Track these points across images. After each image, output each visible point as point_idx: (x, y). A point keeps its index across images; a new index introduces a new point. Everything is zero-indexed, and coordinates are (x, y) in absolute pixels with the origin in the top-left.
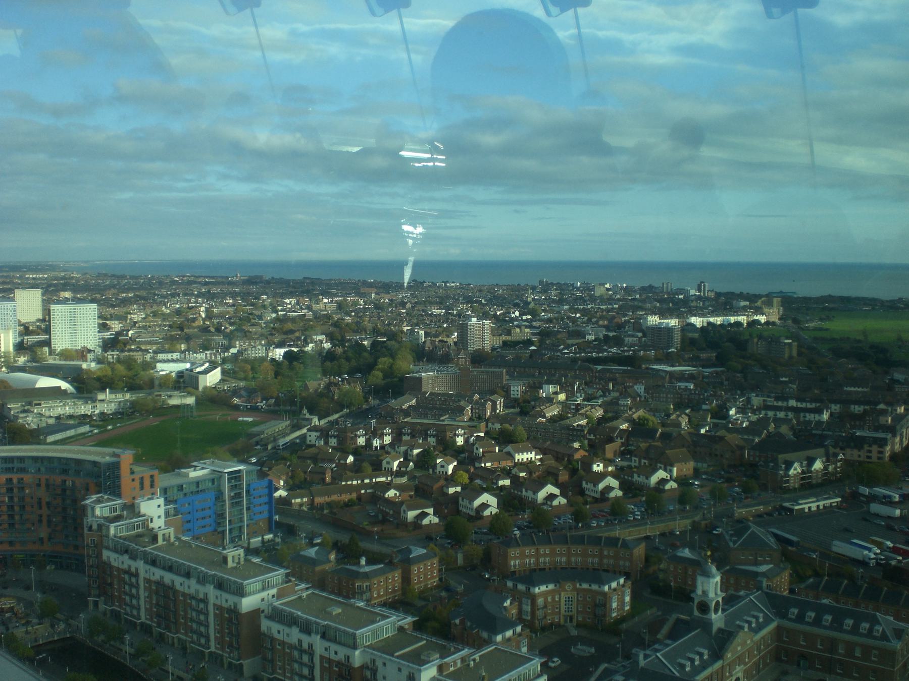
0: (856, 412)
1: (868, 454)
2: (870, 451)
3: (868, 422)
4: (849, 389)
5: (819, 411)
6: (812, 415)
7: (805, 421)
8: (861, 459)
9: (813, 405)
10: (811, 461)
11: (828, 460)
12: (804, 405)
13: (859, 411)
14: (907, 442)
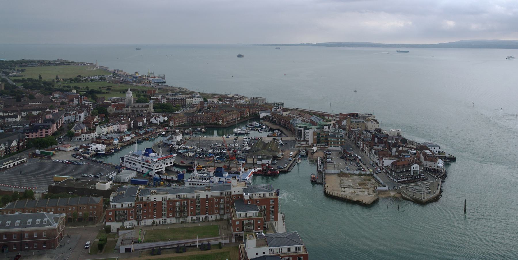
0: (35, 114)
1: (41, 134)
2: (42, 133)
3: (41, 118)
4: (31, 104)
5: (16, 116)
6: (12, 119)
7: (8, 122)
8: (37, 137)
9: (12, 114)
10: (11, 142)
11: (19, 140)
12: (7, 114)
13: (36, 114)
14: (60, 125)
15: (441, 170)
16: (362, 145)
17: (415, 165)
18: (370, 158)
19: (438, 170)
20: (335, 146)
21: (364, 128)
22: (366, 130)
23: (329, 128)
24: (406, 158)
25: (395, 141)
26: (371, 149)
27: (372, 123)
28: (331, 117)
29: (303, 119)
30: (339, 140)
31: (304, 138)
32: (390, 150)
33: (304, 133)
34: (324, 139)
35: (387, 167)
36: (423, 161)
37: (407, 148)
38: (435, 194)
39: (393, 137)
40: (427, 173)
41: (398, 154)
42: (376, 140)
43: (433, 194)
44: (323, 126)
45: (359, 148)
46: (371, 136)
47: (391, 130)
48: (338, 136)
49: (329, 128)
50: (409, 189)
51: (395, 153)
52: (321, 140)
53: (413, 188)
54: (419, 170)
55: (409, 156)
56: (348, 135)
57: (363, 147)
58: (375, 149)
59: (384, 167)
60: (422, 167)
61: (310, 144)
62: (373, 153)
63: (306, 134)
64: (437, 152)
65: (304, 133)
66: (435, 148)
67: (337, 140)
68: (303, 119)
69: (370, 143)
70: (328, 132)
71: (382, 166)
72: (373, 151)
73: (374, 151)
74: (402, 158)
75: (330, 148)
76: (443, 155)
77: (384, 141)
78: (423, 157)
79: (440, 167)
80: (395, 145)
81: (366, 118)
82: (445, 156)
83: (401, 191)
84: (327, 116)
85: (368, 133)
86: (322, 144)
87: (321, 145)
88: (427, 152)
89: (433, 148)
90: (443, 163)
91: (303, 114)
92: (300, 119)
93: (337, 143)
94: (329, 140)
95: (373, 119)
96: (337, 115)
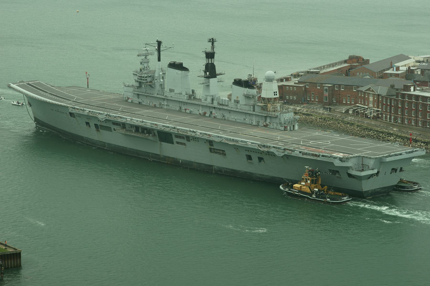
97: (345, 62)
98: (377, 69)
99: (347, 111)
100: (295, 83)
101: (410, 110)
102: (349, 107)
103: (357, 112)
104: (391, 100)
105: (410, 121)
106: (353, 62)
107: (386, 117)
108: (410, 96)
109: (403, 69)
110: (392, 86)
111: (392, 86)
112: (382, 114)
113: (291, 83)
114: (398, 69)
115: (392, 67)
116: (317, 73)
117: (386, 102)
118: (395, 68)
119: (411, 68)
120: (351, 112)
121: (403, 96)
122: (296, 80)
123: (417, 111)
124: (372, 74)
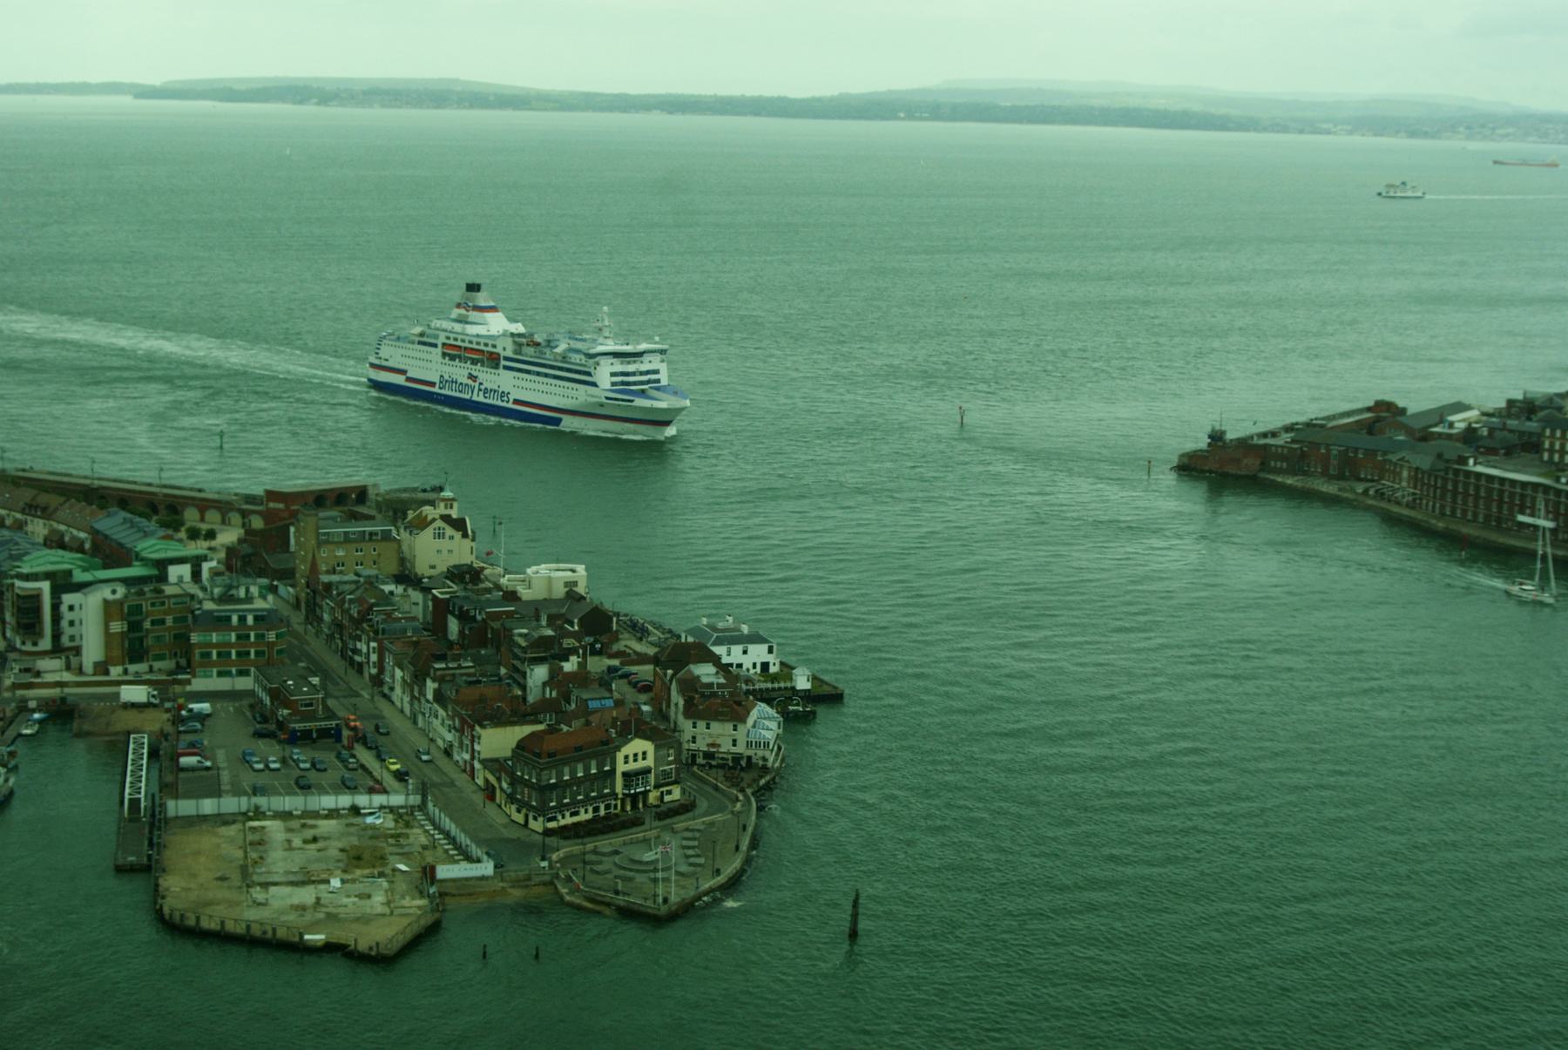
15: (765, 759)
16: (374, 657)
17: (638, 745)
18: (415, 722)
19: (749, 758)
20: (228, 674)
21: (393, 567)
22: (406, 577)
23: (196, 575)
24: (595, 711)
25: (549, 625)
26: (419, 678)
27: (439, 535)
28: (218, 509)
29: (53, 531)
30: (252, 639)
31: (56, 636)
32: (519, 677)
33: (56, 607)
34: (168, 637)
35: (493, 764)
36: (681, 718)
37: (611, 656)
38: (719, 878)
39: (536, 607)
40: (694, 775)
41: (554, 694)
42: (453, 626)
43: (713, 878)
44: (162, 565)
45: (359, 668)
46: (425, 607)
47: (534, 568)
48: (242, 619)
49: (196, 575)
50: (599, 863)
51: (541, 688)
52: (149, 642)
53: (617, 859)
54: (652, 765)
55: (610, 703)
56: (303, 606)
57: (381, 669)
58: (439, 673)
59: (483, 762)
60: (671, 751)
61: (88, 666)
62: (430, 696)
63: (67, 616)
64: (758, 669)
65: (56, 607)
66: (745, 652)
67: (239, 637)
68: (53, 531)
69: (416, 644)
70: (192, 597)
71: (473, 758)
72: (431, 686)
73: (436, 685)
74: (574, 715)
75: (199, 684)
76: (782, 685)
77: (492, 628)
78: (681, 703)
79: (758, 744)
80: (549, 651)
81: (405, 515)
82: (793, 688)
83: (557, 876)
84: (216, 508)
85: (410, 591)
86: (157, 665)
87: (151, 670)
88: (705, 672)
89: (737, 649)
90: (774, 725)
91: (53, 500)
92: (38, 528)
93: (239, 654)
94: (195, 638)
95: (446, 519)
96: (250, 499)
97: (1369, 409)
98: (1417, 425)
99: (1366, 492)
100: (1287, 442)
101: (1466, 494)
102: (1370, 484)
103: (1383, 494)
104: (1436, 477)
105: (1464, 512)
106: (1381, 411)
107: (1427, 505)
108: (1468, 474)
109: (1462, 425)
110: (1440, 456)
111: (1440, 456)
112: (1421, 499)
113: (1279, 441)
114: (1451, 425)
115: (1441, 421)
116: (1322, 426)
117: (1429, 480)
118: (1447, 424)
119: (1474, 425)
120: (1371, 492)
121: (1457, 472)
122: (1287, 437)
123: (1477, 497)
124: (1409, 431)
